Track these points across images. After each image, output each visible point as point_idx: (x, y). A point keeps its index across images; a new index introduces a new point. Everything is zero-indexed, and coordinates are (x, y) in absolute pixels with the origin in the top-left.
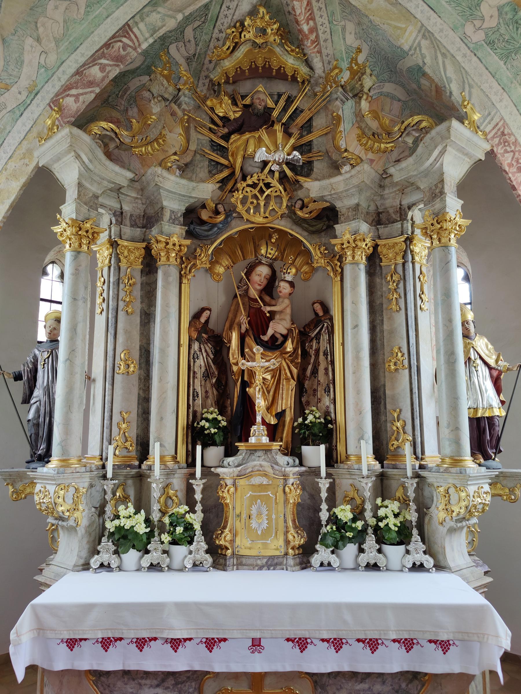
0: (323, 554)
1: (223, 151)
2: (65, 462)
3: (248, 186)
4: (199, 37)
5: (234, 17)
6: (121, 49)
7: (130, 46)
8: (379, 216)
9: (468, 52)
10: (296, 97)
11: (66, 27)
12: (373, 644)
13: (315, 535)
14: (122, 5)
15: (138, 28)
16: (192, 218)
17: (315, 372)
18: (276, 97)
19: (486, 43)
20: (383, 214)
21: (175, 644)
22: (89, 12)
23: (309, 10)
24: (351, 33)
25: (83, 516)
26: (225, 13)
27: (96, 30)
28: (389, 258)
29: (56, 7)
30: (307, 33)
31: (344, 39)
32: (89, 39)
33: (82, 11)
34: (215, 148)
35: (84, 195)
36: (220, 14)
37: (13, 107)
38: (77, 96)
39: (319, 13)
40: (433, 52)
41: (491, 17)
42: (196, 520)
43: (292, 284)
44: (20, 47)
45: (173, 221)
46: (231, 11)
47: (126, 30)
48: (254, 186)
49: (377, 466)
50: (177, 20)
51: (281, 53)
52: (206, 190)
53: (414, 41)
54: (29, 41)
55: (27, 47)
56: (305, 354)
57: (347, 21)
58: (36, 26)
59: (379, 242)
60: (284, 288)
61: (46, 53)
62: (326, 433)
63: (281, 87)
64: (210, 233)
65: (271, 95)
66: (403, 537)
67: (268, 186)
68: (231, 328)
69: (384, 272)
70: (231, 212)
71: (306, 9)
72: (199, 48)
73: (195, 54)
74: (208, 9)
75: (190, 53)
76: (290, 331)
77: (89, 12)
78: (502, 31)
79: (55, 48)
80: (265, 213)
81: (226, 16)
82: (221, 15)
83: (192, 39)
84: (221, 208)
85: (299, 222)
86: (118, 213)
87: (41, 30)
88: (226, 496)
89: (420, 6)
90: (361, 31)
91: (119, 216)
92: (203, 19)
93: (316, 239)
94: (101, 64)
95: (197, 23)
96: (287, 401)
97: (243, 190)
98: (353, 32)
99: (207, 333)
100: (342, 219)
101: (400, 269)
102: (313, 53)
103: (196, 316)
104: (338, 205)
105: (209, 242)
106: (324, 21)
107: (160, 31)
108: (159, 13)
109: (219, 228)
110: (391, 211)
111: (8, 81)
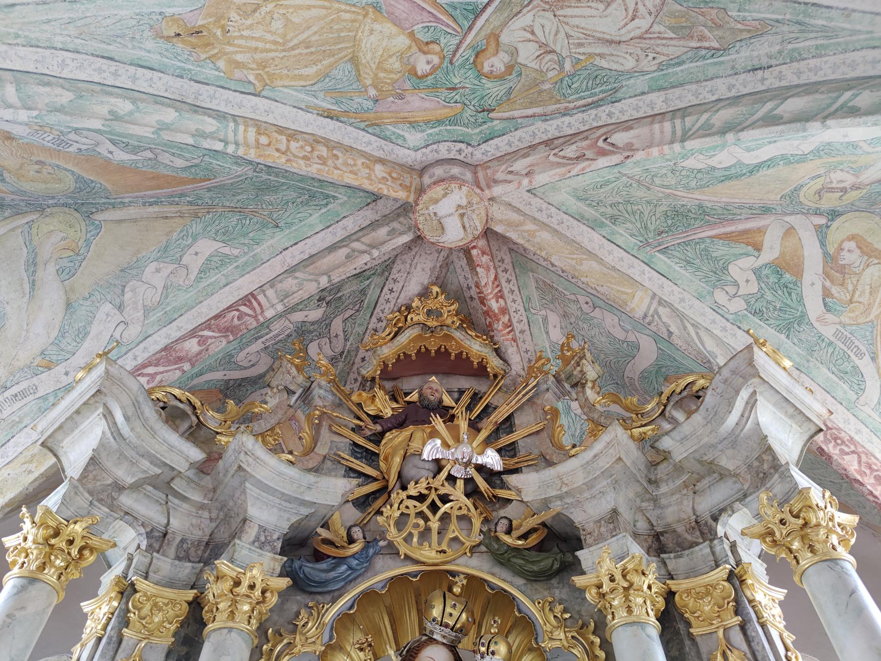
1: (371, 457)
3: (410, 497)
4: (350, 329)
5: (399, 301)
6: (235, 319)
7: (249, 315)
8: (658, 540)
9: (728, 325)
10: (485, 393)
11: (164, 294)
14: (248, 273)
15: (265, 295)
18: (456, 395)
19: (750, 313)
20: (666, 535)
22: (201, 278)
23: (498, 286)
24: (555, 327)
26: (387, 297)
27: (205, 299)
29: (158, 271)
30: (496, 311)
31: (547, 333)
32: (194, 310)
33: (192, 277)
34: (359, 455)
35: (95, 478)
36: (381, 299)
37: (47, 392)
38: (153, 376)
39: (511, 297)
40: (679, 321)
41: (747, 281)
44: (91, 314)
45: (261, 543)
46: (395, 295)
47: (248, 300)
48: (421, 498)
50: (319, 284)
51: (462, 338)
53: (649, 308)
54: (107, 307)
55: (101, 315)
57: (548, 311)
58: (123, 291)
59: (673, 585)
61: (126, 324)
63: (464, 383)
64: (333, 574)
65: (450, 392)
67: (445, 499)
69: (704, 649)
70: (376, 546)
71: (493, 283)
72: (349, 343)
73: (343, 352)
74: (366, 295)
75: (337, 351)
77: (201, 278)
78: (769, 296)
79: (142, 319)
80: (439, 544)
81: (388, 301)
82: (382, 300)
83: (341, 333)
84: (357, 533)
85: (503, 557)
86: (157, 534)
87: (128, 295)
89: (646, 273)
90: (568, 326)
91: (158, 539)
92: (356, 308)
93: (543, 592)
94: (202, 336)
95: (349, 313)
98: (558, 326)
100: (590, 540)
101: (737, 637)
102: (507, 340)
104: (578, 517)
105: (328, 598)
106: (519, 308)
107: (295, 295)
108: (296, 278)
109: (350, 568)
110: (680, 529)
111: (54, 358)
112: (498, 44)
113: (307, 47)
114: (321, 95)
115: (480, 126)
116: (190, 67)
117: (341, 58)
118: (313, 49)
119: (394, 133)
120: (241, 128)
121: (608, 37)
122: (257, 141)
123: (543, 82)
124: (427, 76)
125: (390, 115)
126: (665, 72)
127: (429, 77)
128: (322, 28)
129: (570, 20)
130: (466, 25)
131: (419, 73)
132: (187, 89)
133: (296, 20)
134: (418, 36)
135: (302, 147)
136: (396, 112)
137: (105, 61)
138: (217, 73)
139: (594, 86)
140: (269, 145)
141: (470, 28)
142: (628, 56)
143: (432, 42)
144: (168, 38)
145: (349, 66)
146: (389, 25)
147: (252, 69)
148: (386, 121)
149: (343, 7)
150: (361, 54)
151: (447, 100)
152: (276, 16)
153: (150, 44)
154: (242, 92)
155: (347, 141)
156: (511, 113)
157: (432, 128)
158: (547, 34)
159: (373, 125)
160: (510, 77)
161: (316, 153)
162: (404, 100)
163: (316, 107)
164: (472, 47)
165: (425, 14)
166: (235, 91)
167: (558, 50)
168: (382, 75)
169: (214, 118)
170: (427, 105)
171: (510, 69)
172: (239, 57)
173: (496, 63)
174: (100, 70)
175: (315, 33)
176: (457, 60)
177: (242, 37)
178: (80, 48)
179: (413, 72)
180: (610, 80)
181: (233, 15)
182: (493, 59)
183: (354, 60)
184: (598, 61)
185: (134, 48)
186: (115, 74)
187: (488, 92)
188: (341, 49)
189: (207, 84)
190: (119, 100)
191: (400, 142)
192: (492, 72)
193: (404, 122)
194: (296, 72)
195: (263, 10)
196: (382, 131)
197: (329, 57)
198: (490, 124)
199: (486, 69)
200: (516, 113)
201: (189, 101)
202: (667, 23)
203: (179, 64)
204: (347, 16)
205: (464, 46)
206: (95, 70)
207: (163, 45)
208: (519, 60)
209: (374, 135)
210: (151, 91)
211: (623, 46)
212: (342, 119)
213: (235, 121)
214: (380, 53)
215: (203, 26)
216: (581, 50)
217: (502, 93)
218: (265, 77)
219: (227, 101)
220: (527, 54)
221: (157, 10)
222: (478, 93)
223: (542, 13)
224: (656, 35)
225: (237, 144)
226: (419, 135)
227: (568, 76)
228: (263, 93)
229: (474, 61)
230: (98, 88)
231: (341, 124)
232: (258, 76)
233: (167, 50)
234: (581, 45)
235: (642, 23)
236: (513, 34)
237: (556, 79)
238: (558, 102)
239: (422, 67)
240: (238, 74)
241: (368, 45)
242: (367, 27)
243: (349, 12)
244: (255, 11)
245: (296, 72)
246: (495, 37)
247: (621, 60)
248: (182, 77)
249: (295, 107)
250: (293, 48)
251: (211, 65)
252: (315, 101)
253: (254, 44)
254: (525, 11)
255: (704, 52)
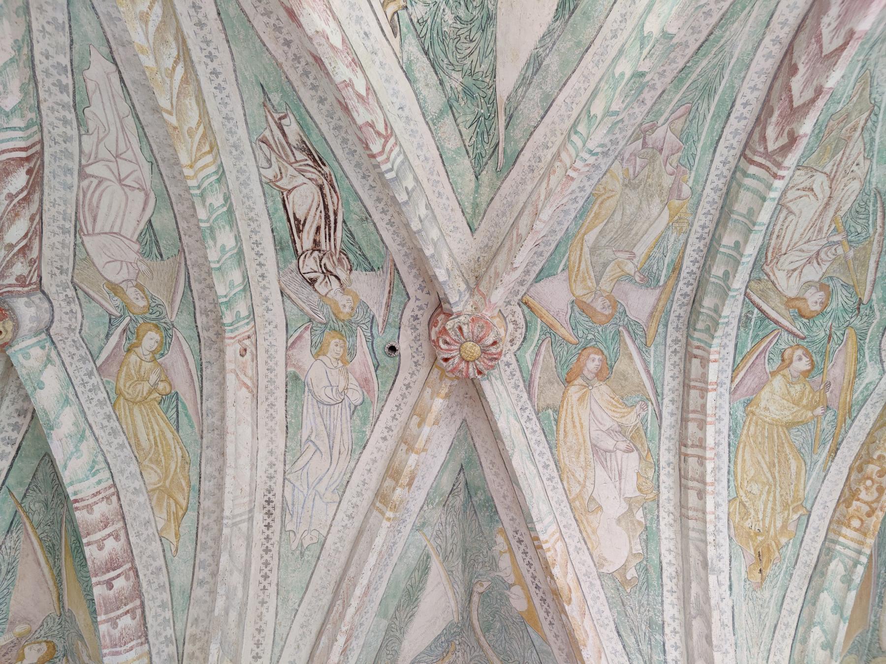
112: (797, 299)
113: (774, 466)
114: (815, 457)
115: (873, 311)
116: (785, 566)
117: (786, 437)
118: (776, 461)
119: (862, 392)
120: (841, 539)
121: (821, 208)
122: (856, 530)
123: (845, 257)
124: (813, 361)
125: (843, 395)
126: (876, 153)
127: (814, 359)
128: (760, 451)
129: (794, 241)
130: (773, 326)
131: (809, 368)
132: (802, 572)
133: (752, 472)
134: (775, 368)
135: (867, 489)
136: (841, 390)
137: (777, 632)
138: (790, 546)
139: (866, 212)
140: (861, 520)
141: (776, 322)
142: (846, 188)
143: (782, 356)
144: (763, 579)
145: (793, 431)
146: (763, 393)
147: (789, 515)
148: (848, 399)
149: (745, 432)
150: (785, 420)
151: (840, 342)
152: (749, 489)
153: (767, 594)
154: (807, 527)
155: (862, 438)
156: (868, 283)
157: (864, 356)
158: (797, 259)
159: (850, 412)
160: (831, 286)
161: (874, 476)
162: (832, 382)
163: (825, 463)
164: (793, 320)
165: (757, 362)
166: (805, 532)
167: (817, 248)
168: (805, 402)
169: (831, 560)
170: (840, 361)
171: (822, 286)
172: (779, 524)
173: (814, 300)
174: (784, 637)
175: (763, 457)
176: (802, 333)
177: (763, 520)
178: (767, 648)
179: (806, 374)
180: (865, 200)
181: (747, 524)
182: (809, 303)
183: (789, 426)
184: (841, 213)
185: (768, 607)
186: (787, 625)
187: (840, 305)
188: (778, 436)
189: (798, 555)
190: (812, 636)
191: (872, 387)
192: (822, 303)
193: (853, 383)
194: (793, 477)
195: (744, 499)
196: (857, 404)
197: (783, 447)
198: (874, 303)
199: (818, 308)
200: (870, 278)
201: (810, 573)
202: (827, 160)
203: (782, 575)
204: (752, 429)
205: (791, 327)
206: (783, 641)
207: (767, 584)
208: (817, 279)
209: (859, 411)
210: (801, 601)
211: (835, 194)
212: (840, 440)
213: (835, 542)
214: (785, 402)
215: (755, 550)
216: (826, 228)
217: (845, 292)
218: (795, 504)
219: (813, 540)
220: (813, 273)
221: (743, 583)
222: (840, 314)
223: (779, 264)
224: (835, 168)
225: (860, 553)
226: (869, 369)
227: (848, 236)
228: (808, 507)
229: (808, 318)
230: (798, 646)
231: (845, 442)
232: (795, 511)
233: (771, 582)
234: (820, 230)
235: (820, 182)
236: (789, 287)
237: (847, 247)
238: (871, 243)
239: (803, 365)
240: (792, 527)
241: (777, 413)
242: (763, 413)
243: (749, 427)
244: (744, 506)
245: (793, 477)
246: (789, 302)
247: (849, 193)
248: (792, 574)
249: (823, 482)
250: (774, 478)
251: (784, 549)
252: (819, 463)
253: (769, 510)
254: (772, 278)
255: (869, 124)
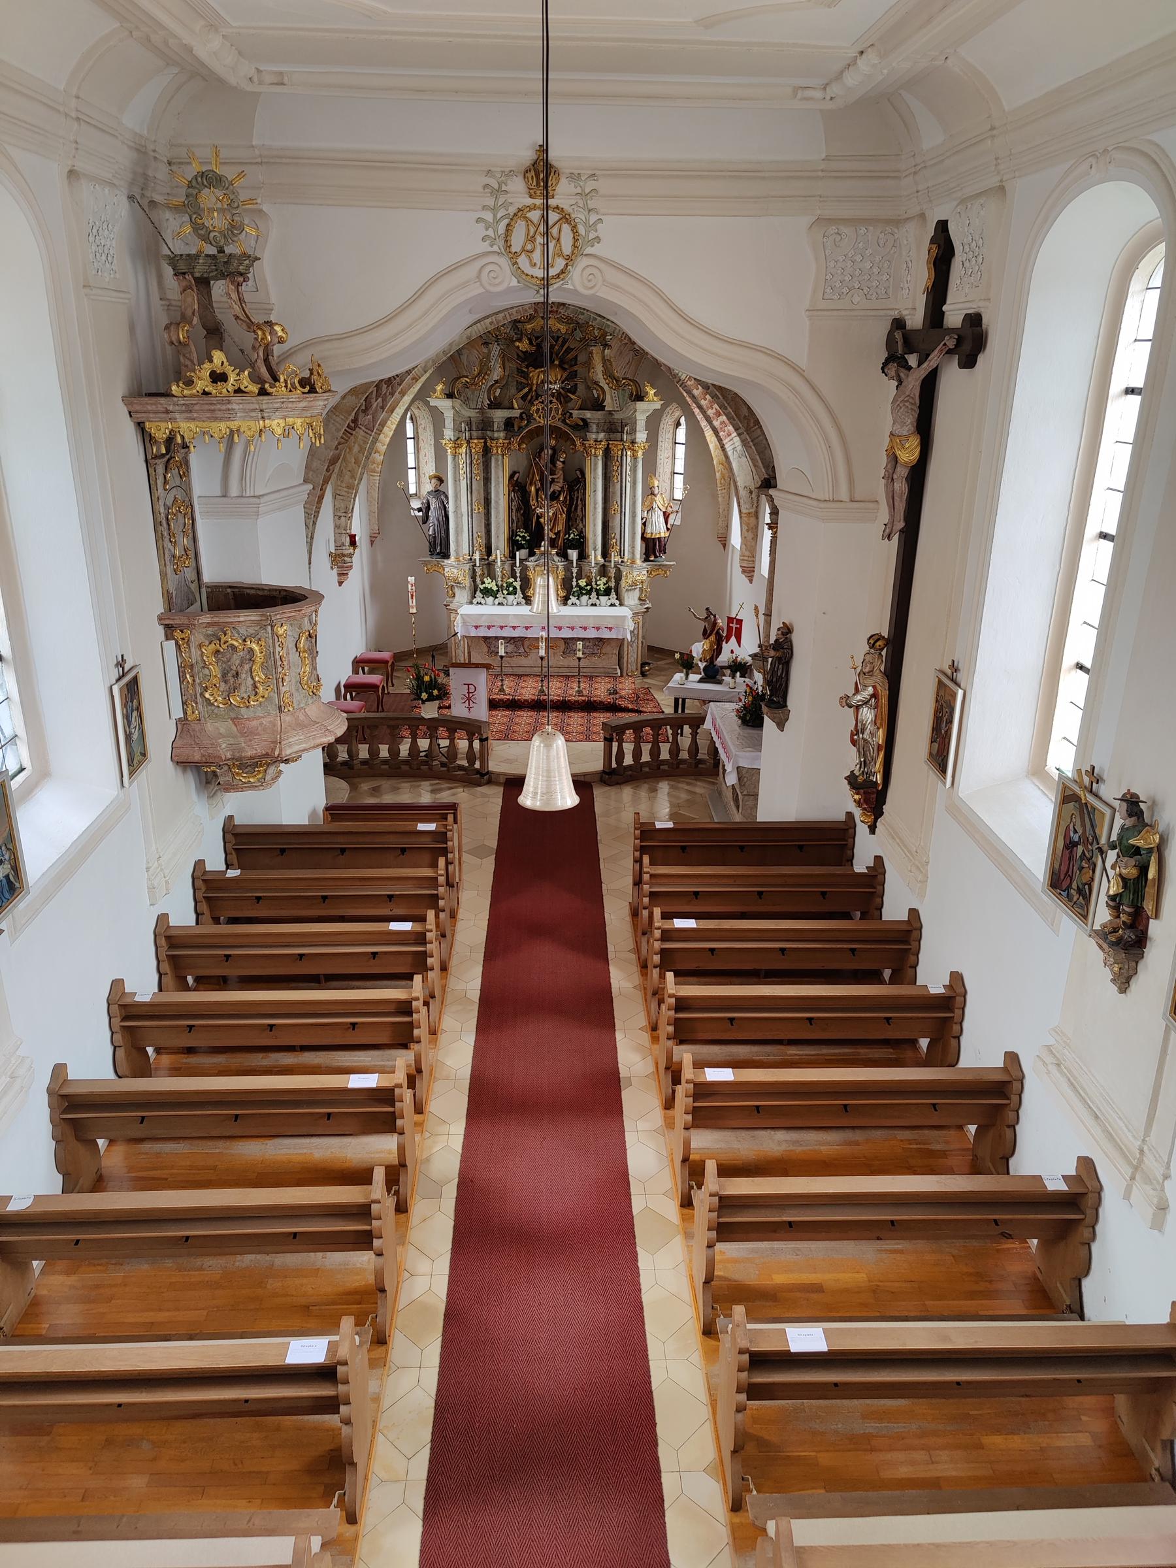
0: (573, 599)
2: (457, 559)
12: (585, 629)
13: (568, 592)
16: (509, 424)
17: (576, 509)
21: (514, 628)
25: (468, 582)
28: (616, 452)
42: (517, 584)
43: (563, 462)
49: (602, 561)
52: (516, 413)
56: (571, 499)
60: (559, 465)
62: (580, 544)
66: (607, 592)
67: (551, 402)
68: (531, 484)
70: (530, 418)
76: (562, 488)
88: (530, 574)
93: (578, 433)
96: (560, 527)
97: (537, 405)
99: (518, 487)
103: (511, 477)
